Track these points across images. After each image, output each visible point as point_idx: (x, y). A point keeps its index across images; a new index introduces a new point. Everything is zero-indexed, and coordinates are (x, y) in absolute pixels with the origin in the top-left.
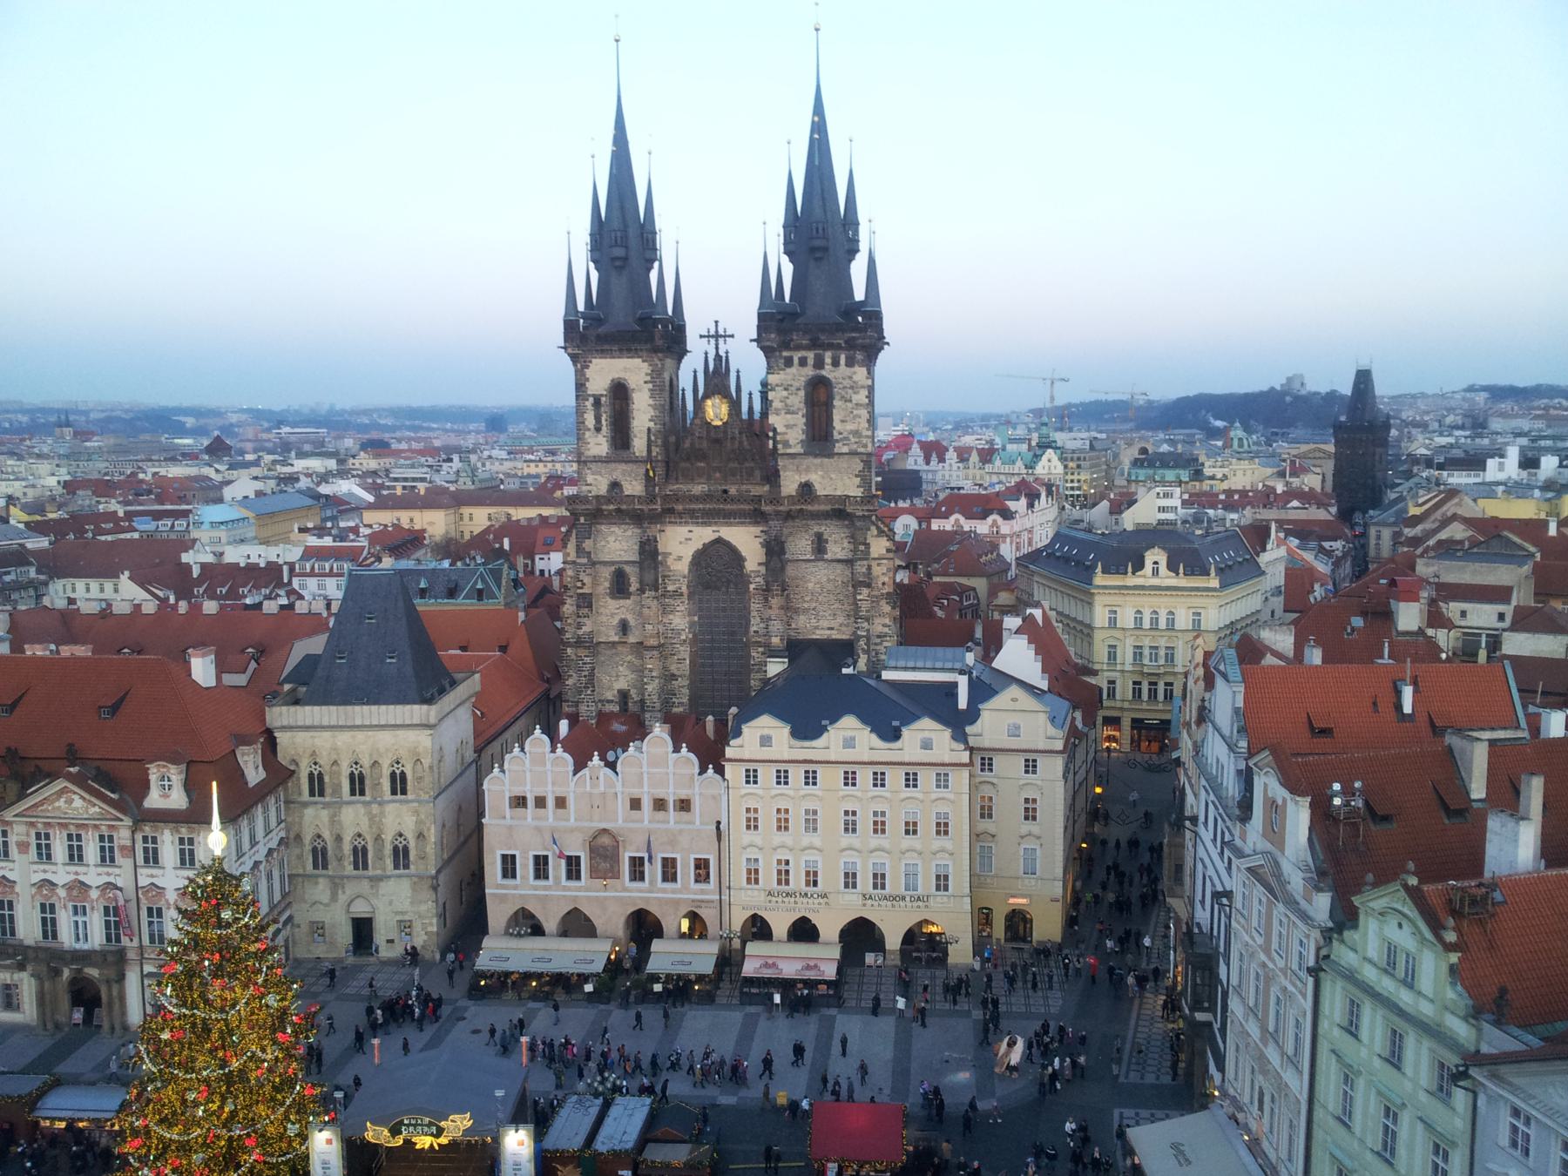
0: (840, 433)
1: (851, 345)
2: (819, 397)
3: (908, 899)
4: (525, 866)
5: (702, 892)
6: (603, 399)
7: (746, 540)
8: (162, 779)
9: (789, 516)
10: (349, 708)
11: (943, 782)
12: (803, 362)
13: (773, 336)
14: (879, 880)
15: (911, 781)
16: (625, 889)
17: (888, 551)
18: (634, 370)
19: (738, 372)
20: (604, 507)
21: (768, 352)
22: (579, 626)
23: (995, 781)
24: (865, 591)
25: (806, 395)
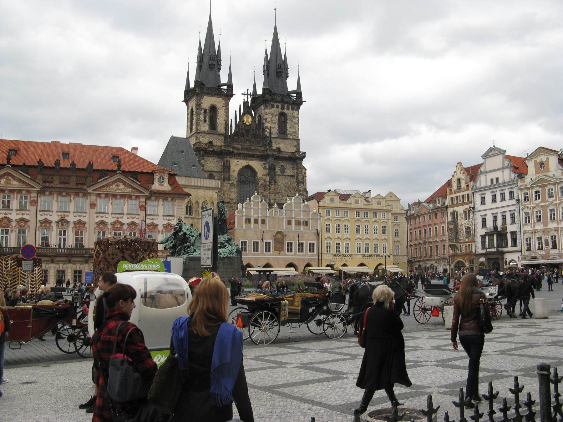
0: (290, 132)
2: (283, 119)
3: (376, 256)
4: (250, 246)
5: (312, 255)
6: (207, 111)
7: (257, 165)
8: (160, 178)
10: (190, 178)
12: (277, 107)
14: (367, 249)
16: (286, 255)
18: (218, 102)
20: (208, 149)
24: (302, 185)
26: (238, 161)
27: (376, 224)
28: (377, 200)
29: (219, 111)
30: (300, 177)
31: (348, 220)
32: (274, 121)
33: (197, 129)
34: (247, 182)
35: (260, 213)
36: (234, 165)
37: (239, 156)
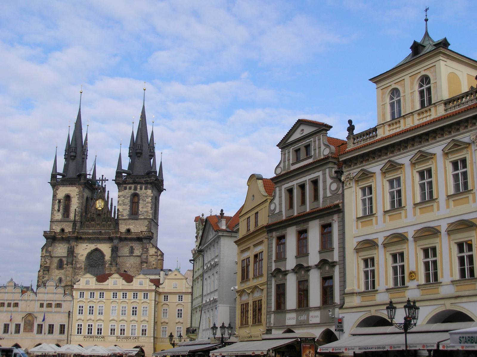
1: (146, 183)
2: (135, 199)
3: (132, 338)
6: (62, 200)
7: (106, 249)
9: (121, 239)
11: (146, 296)
12: (130, 188)
13: (120, 179)
14: (123, 331)
15: (135, 296)
17: (156, 252)
18: (73, 191)
19: (108, 191)
20: (57, 237)
21: (118, 184)
22: (43, 278)
23: (168, 303)
26: (87, 246)
28: (139, 280)
30: (144, 256)
31: (103, 301)
32: (126, 203)
33: (51, 219)
34: (96, 265)
36: (83, 250)
37: (88, 241)
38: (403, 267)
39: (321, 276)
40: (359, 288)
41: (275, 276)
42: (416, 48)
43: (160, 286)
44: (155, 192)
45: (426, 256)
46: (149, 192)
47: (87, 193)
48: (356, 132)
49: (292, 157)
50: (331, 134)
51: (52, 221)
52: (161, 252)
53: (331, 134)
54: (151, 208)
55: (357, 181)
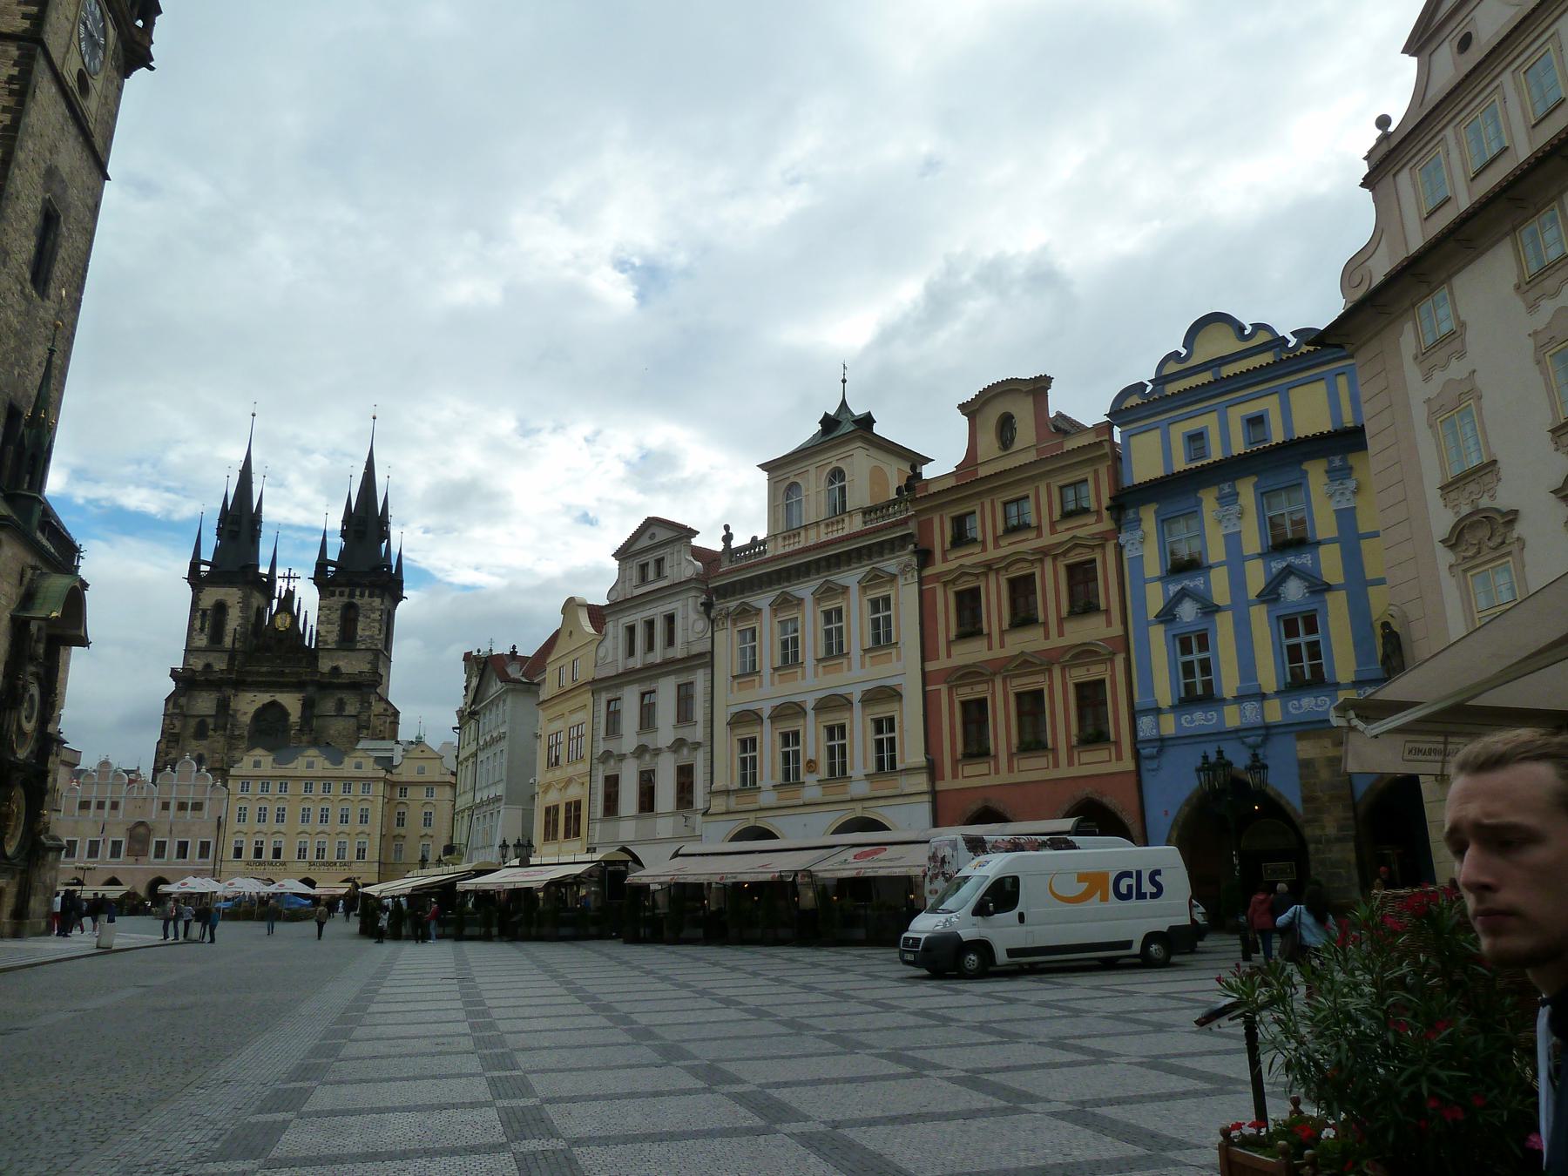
0: (361, 637)
3: (338, 864)
5: (203, 864)
6: (209, 612)
7: (291, 702)
12: (341, 594)
14: (320, 852)
15: (347, 789)
16: (150, 863)
17: (386, 710)
18: (232, 596)
19: (300, 598)
22: (167, 755)
23: (407, 802)
24: (365, 732)
25: (342, 613)
27: (345, 805)
28: (355, 760)
29: (230, 610)
30: (364, 717)
31: (285, 799)
35: (109, 791)
38: (797, 753)
39: (675, 763)
40: (731, 784)
41: (603, 763)
42: (829, 423)
43: (393, 771)
44: (387, 602)
45: (831, 737)
46: (377, 602)
47: (257, 600)
48: (735, 544)
49: (635, 573)
50: (696, 542)
51: (189, 648)
52: (395, 709)
53: (696, 542)
54: (380, 630)
55: (734, 622)
